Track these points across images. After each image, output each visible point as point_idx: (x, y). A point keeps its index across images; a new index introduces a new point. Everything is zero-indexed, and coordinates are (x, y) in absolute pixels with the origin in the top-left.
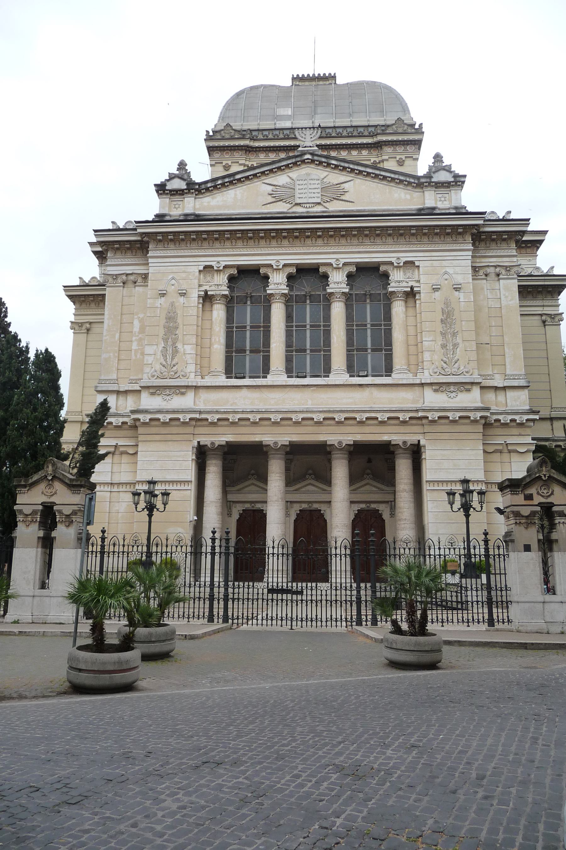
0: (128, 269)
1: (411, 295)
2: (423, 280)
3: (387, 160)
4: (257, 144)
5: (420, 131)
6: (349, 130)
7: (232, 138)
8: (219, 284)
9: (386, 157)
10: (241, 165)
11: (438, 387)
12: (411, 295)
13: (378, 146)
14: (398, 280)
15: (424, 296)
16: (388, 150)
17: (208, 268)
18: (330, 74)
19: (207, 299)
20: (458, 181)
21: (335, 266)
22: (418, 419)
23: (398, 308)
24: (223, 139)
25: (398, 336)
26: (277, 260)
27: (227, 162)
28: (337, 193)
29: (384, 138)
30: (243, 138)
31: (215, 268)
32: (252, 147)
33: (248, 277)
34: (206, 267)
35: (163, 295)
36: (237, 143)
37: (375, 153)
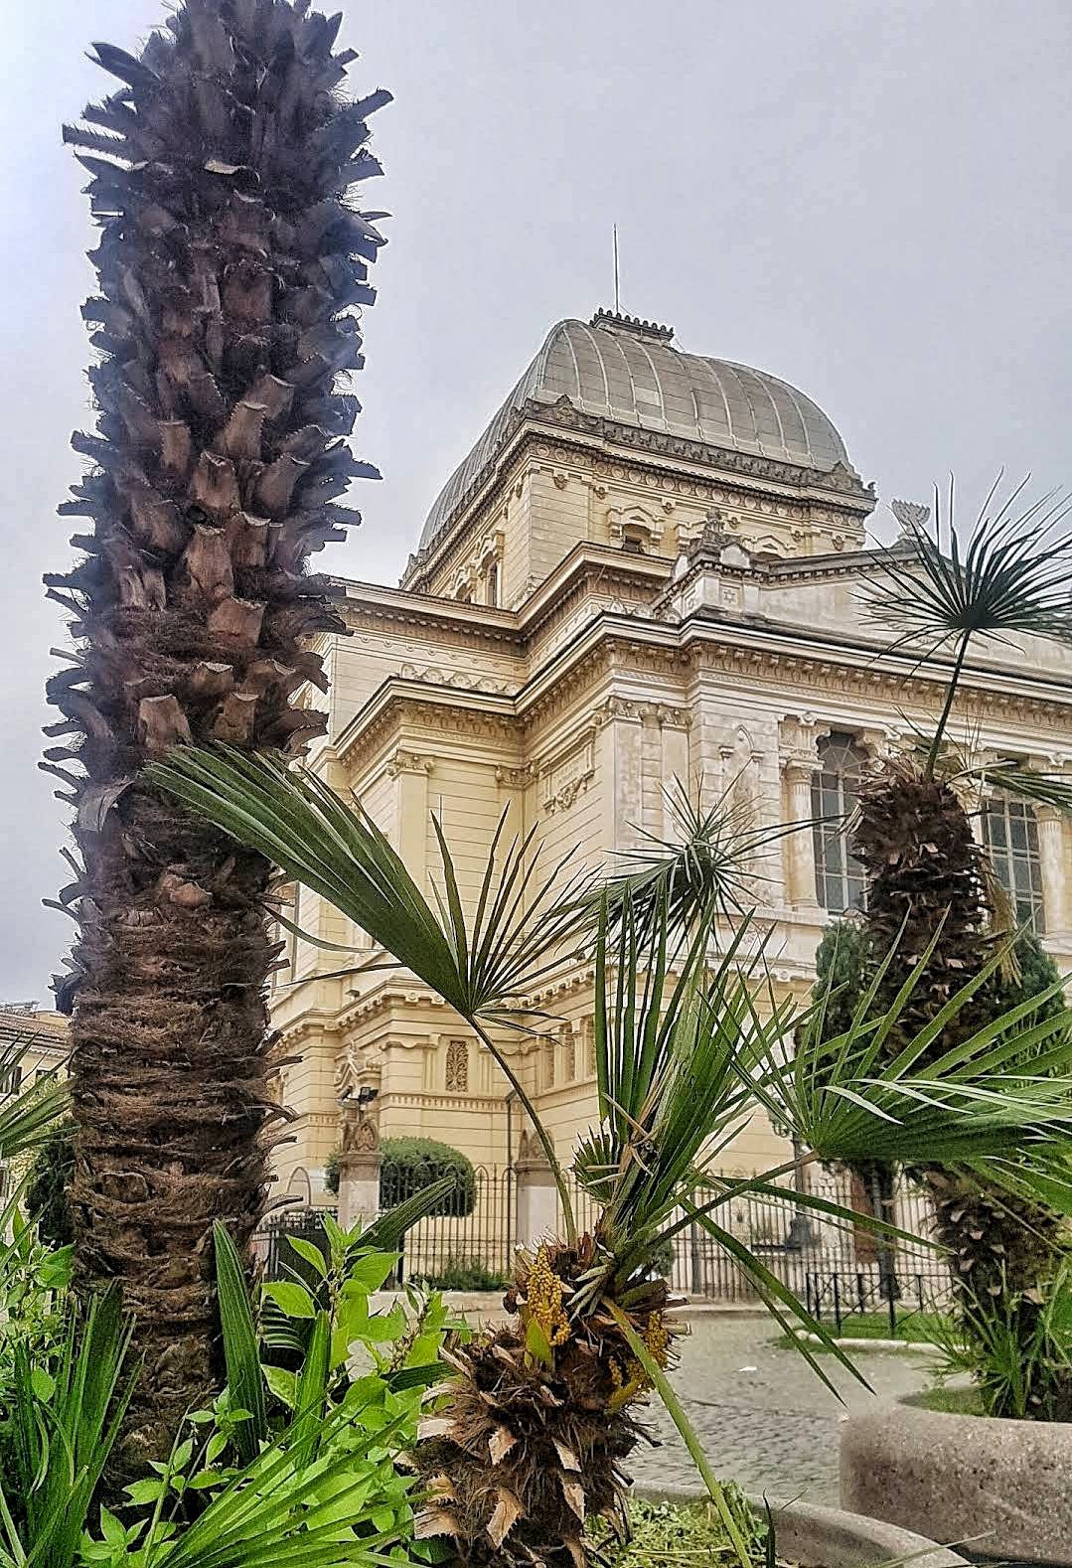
0: (656, 696)
3: (818, 535)
4: (613, 451)
5: (869, 495)
6: (729, 457)
7: (573, 428)
9: (818, 530)
10: (584, 483)
13: (805, 505)
16: (821, 516)
18: (664, 327)
19: (786, 772)
21: (803, 722)
24: (557, 424)
27: (669, 500)
29: (819, 495)
30: (591, 431)
31: (803, 722)
32: (604, 455)
34: (788, 717)
35: (727, 755)
36: (583, 440)
37: (797, 516)
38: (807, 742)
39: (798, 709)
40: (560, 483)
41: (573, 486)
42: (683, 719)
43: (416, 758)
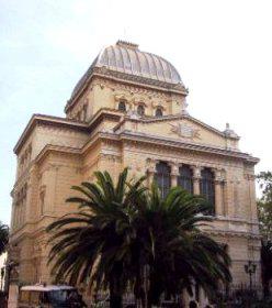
1: (223, 183)
2: (229, 178)
8: (153, 168)
11: (234, 222)
12: (223, 183)
13: (170, 94)
14: (219, 177)
15: (228, 184)
17: (149, 160)
20: (236, 139)
22: (228, 235)
23: (218, 187)
25: (219, 198)
26: (176, 160)
28: (195, 135)
33: (163, 165)
38: (153, 165)
39: (151, 157)
40: (102, 88)
41: (105, 89)
42: (120, 159)
43: (53, 166)
